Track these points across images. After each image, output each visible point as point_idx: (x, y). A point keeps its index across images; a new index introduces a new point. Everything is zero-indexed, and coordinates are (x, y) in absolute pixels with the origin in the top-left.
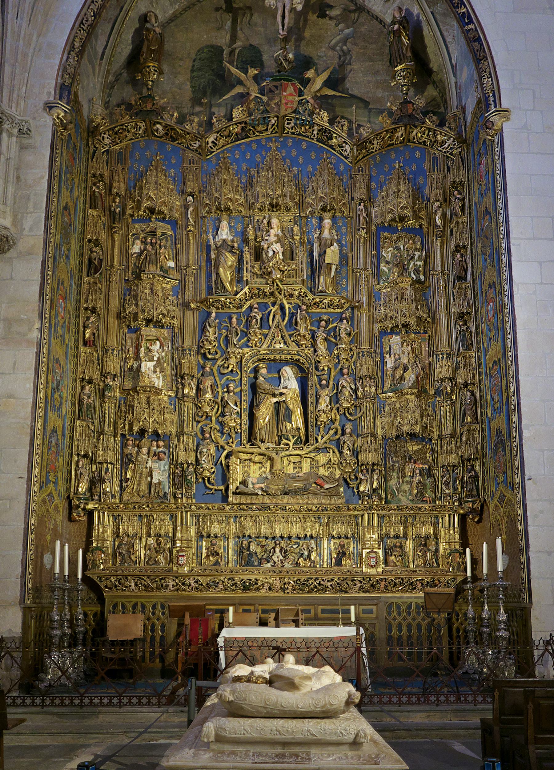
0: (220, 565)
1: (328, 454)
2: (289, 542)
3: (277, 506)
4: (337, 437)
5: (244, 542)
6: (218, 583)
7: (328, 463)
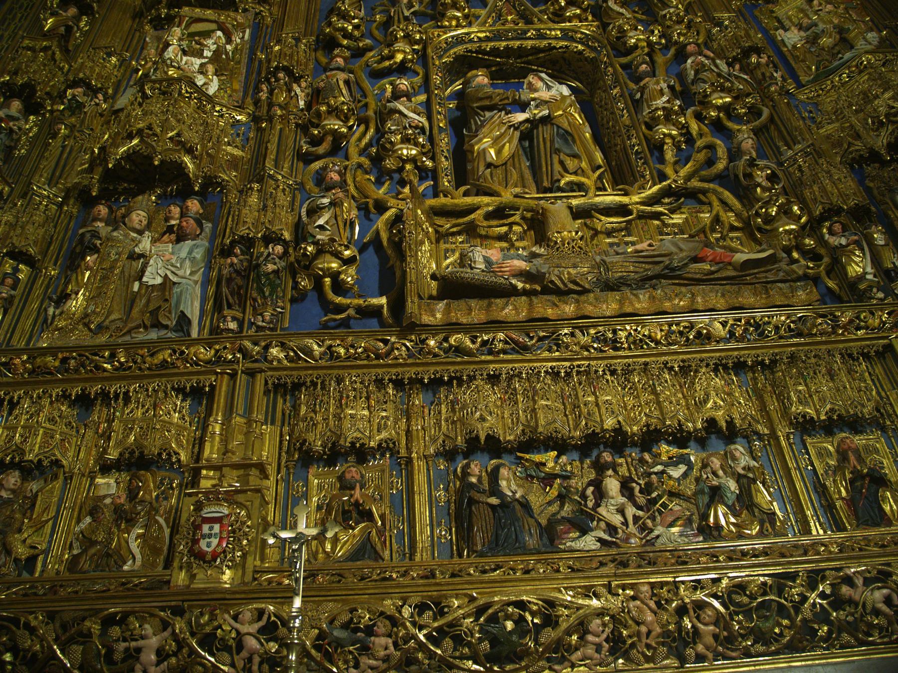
0: (378, 557)
2: (647, 456)
4: (721, 165)
5: (475, 468)
6: (370, 631)
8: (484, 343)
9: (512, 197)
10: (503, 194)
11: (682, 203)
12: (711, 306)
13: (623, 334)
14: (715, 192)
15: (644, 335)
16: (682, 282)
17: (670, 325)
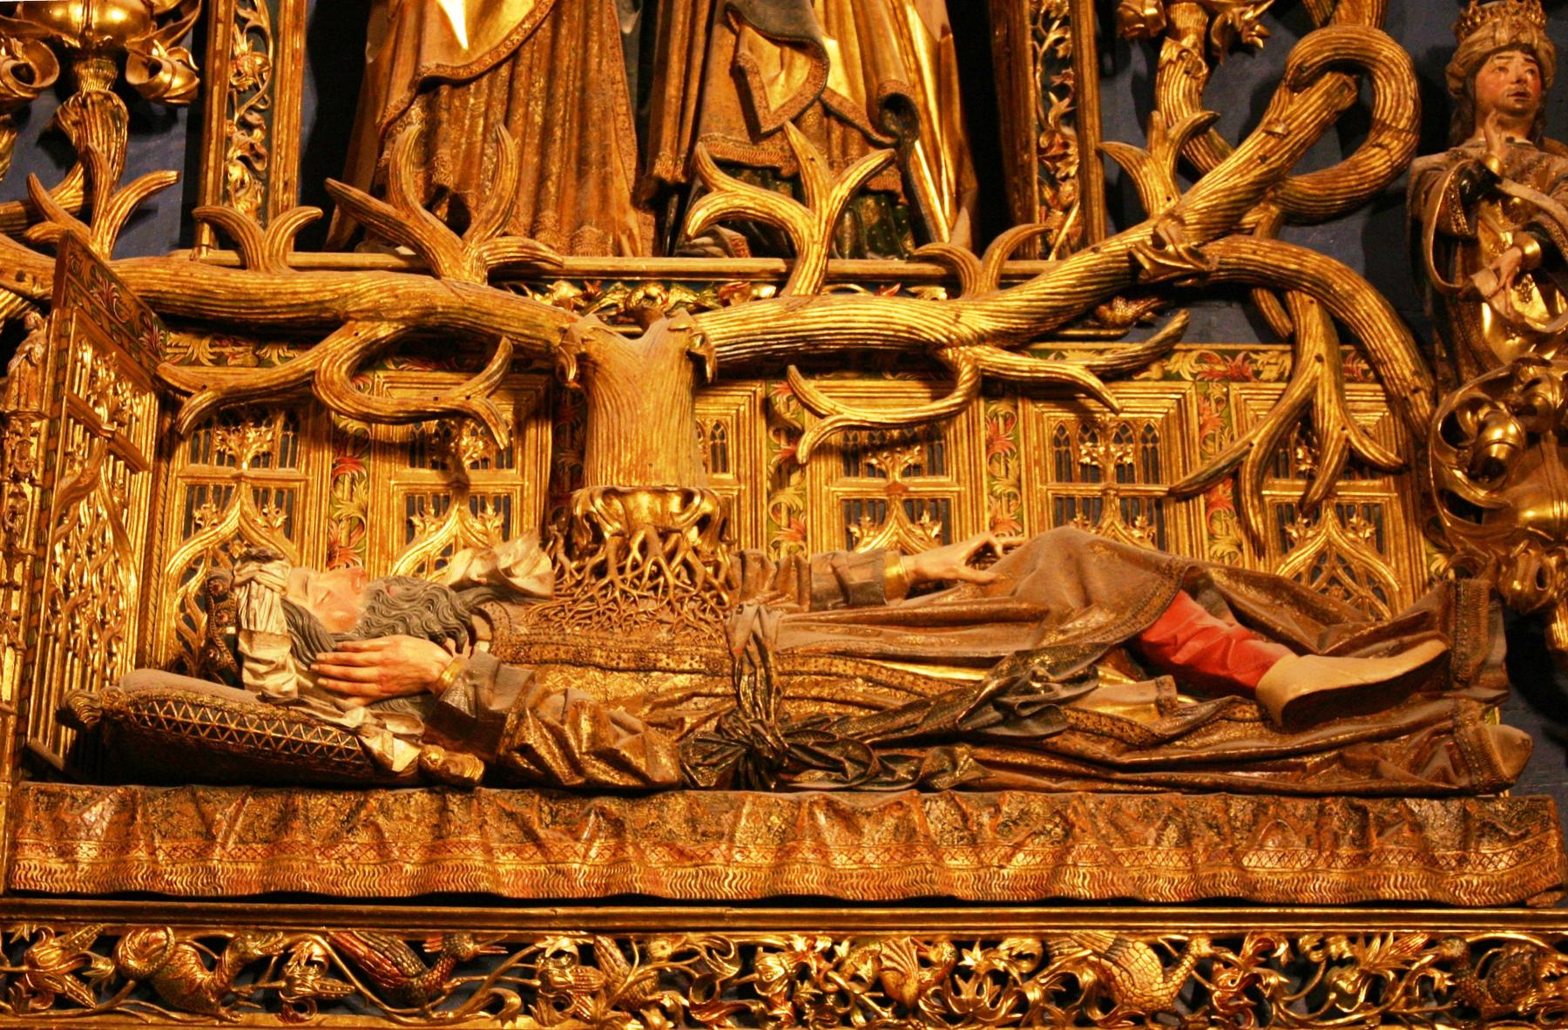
1: (1271, 360)
3: (631, 941)
4: (1376, 160)
7: (1276, 461)
8: (252, 968)
9: (478, 281)
10: (445, 263)
11: (1177, 337)
12: (1125, 890)
13: (775, 967)
14: (1321, 291)
15: (856, 978)
16: (1043, 762)
17: (961, 945)
